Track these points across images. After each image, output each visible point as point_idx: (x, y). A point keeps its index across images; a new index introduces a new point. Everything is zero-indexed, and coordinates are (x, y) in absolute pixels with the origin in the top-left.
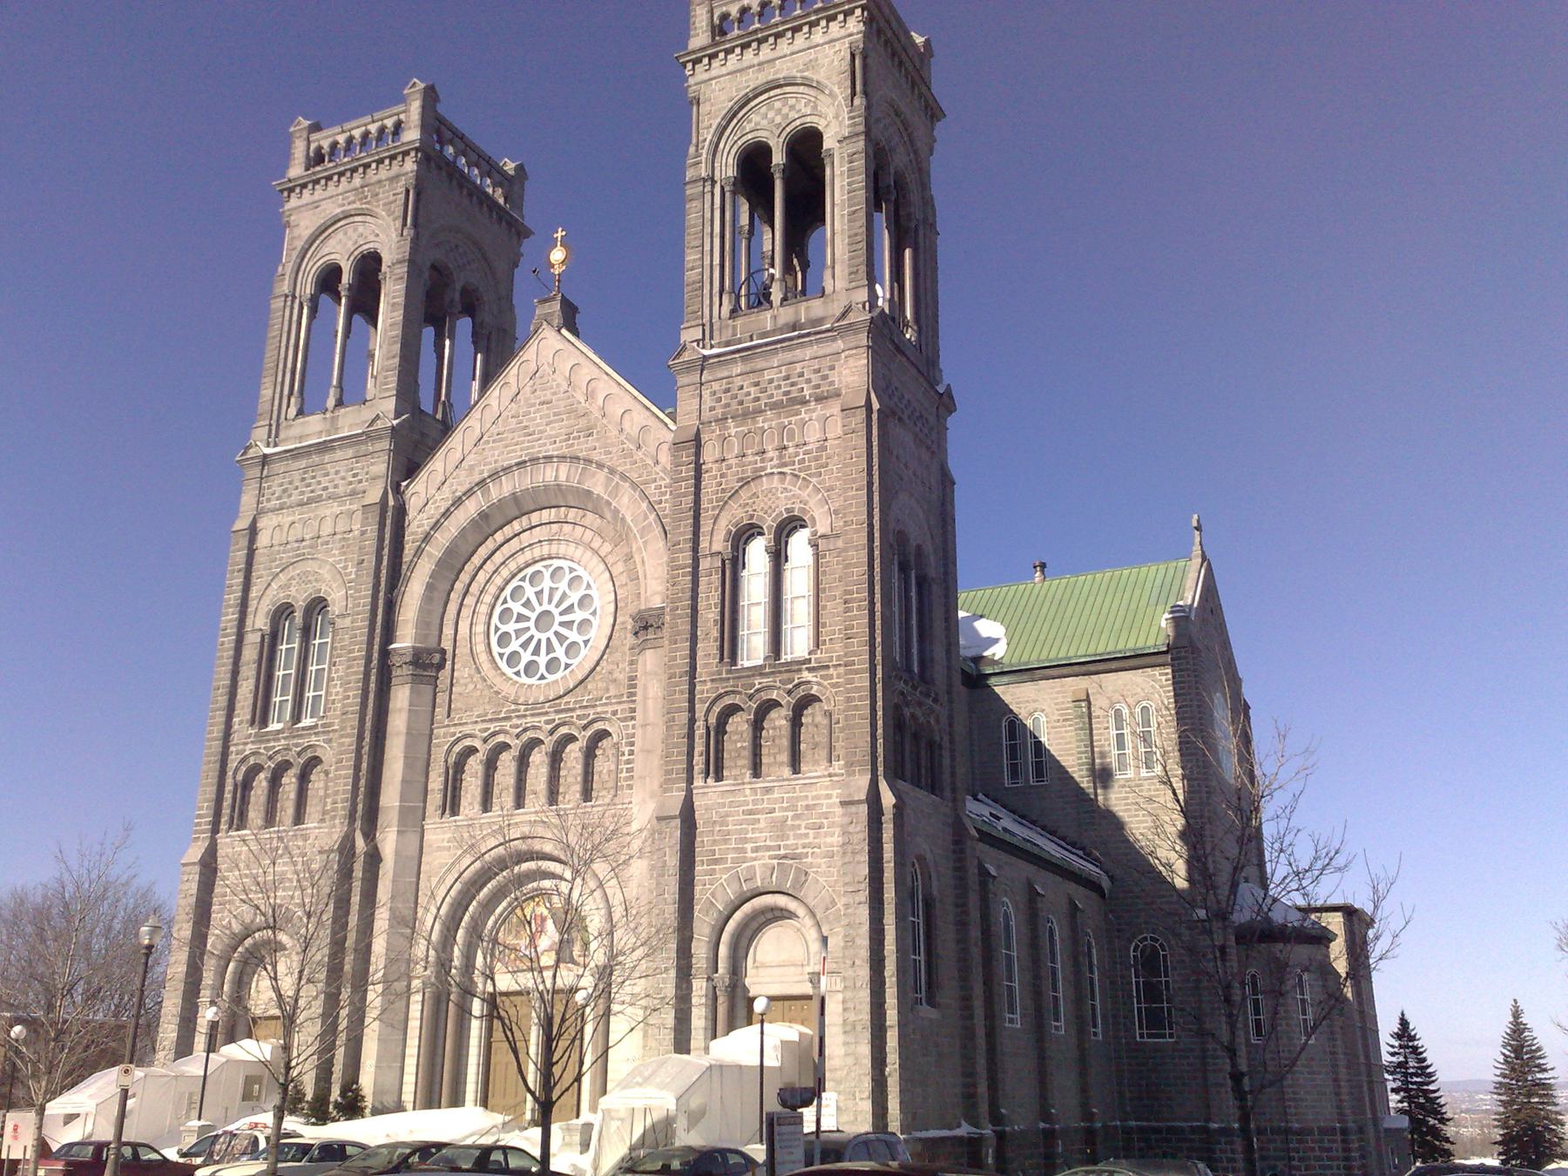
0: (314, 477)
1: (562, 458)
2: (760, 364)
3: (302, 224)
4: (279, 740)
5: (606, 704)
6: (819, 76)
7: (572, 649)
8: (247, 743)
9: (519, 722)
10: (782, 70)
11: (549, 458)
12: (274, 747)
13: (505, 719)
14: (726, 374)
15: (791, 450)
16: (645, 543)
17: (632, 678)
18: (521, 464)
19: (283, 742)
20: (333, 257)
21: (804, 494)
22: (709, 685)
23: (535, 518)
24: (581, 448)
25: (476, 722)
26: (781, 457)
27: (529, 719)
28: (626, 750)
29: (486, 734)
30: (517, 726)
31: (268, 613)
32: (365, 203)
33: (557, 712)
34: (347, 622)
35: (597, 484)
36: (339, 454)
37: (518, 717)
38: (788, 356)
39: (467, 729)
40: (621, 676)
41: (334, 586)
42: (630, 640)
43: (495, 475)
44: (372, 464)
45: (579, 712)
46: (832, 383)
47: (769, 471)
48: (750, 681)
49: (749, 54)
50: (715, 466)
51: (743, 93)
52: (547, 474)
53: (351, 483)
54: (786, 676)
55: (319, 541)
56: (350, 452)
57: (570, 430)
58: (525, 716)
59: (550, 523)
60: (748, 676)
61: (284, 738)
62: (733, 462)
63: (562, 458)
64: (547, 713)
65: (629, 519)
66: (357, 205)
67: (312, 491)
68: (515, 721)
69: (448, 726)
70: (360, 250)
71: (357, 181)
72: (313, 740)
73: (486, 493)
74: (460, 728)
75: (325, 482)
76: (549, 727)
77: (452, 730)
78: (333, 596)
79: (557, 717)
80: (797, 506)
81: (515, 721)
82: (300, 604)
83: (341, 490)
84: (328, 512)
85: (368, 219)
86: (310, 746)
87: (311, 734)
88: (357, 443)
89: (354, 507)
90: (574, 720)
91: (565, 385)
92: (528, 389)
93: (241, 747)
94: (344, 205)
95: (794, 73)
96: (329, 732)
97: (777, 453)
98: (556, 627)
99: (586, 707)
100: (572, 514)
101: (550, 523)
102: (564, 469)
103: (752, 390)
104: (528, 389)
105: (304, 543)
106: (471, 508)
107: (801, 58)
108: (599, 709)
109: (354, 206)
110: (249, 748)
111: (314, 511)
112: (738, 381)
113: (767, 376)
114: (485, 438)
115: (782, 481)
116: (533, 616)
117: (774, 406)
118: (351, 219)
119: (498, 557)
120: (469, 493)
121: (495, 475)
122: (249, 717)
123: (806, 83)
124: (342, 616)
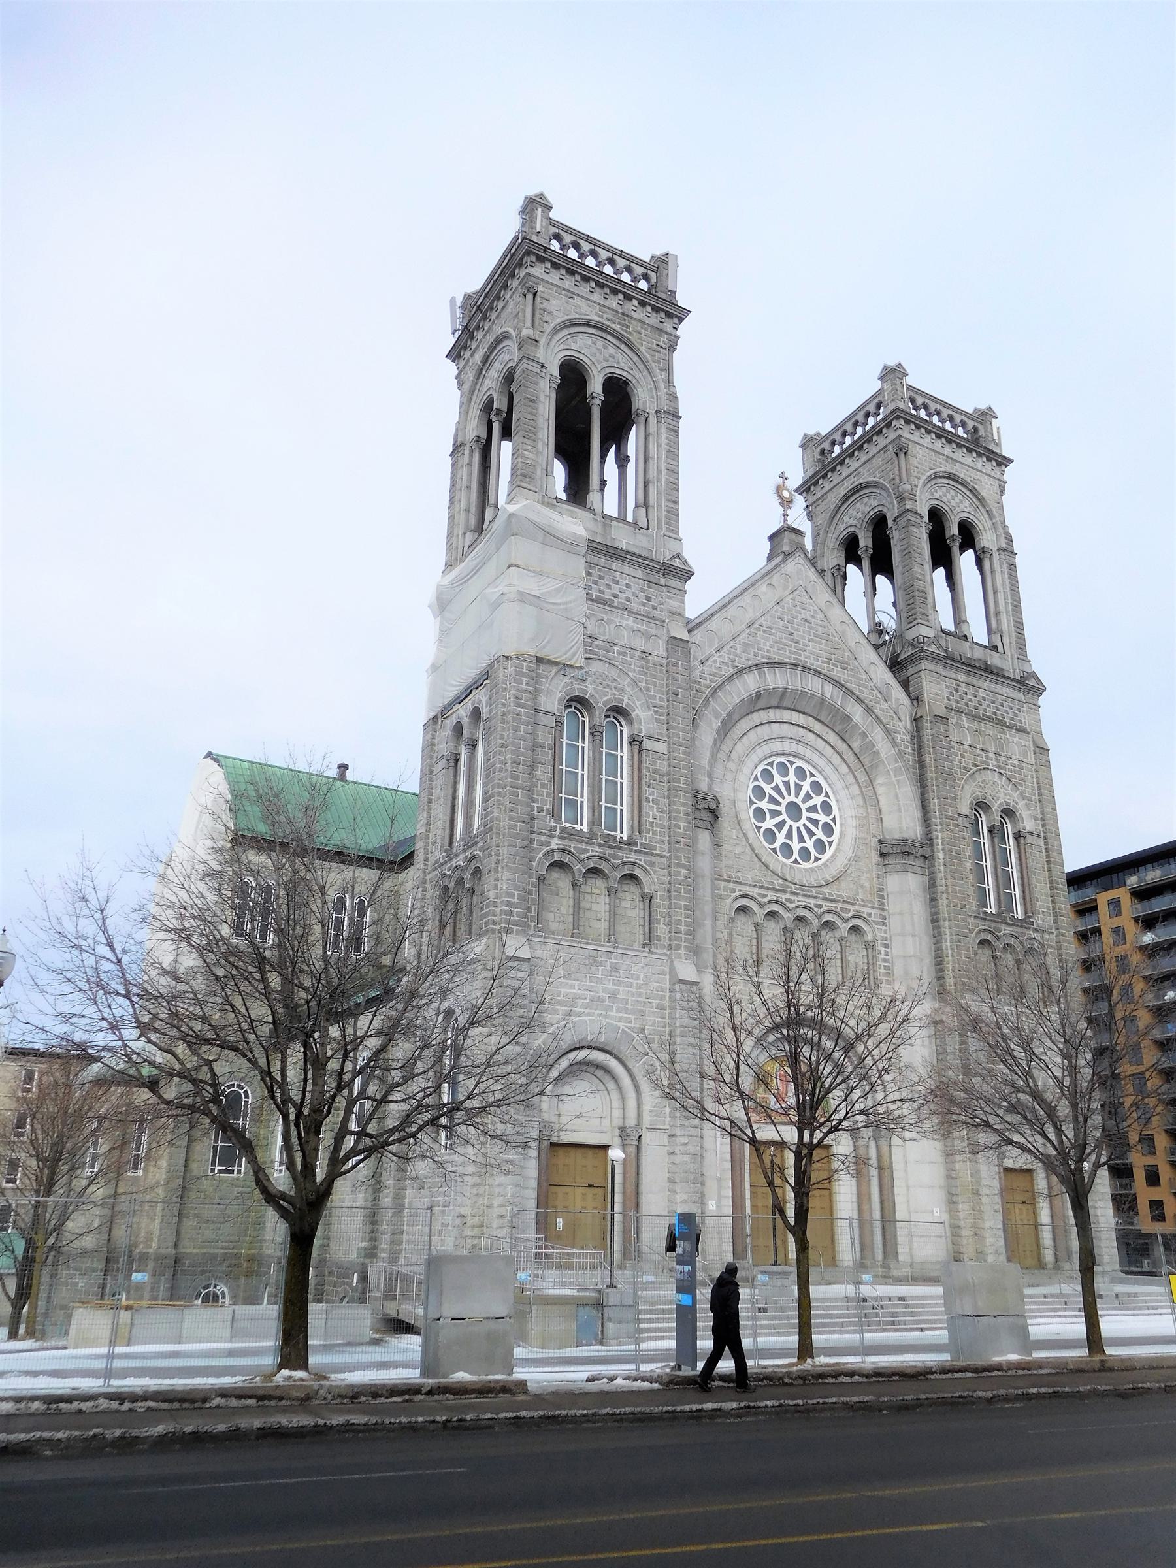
0: (601, 578)
1: (828, 679)
2: (976, 682)
3: (554, 302)
4: (593, 844)
5: (864, 906)
6: (984, 493)
7: (770, 835)
8: (554, 836)
9: (793, 898)
10: (962, 473)
11: (817, 673)
12: (587, 851)
13: (781, 891)
14: (954, 676)
15: (1003, 758)
16: (898, 781)
17: (881, 890)
18: (794, 665)
19: (597, 848)
20: (581, 357)
21: (1016, 795)
22: (972, 920)
23: (787, 715)
24: (837, 673)
25: (755, 886)
26: (997, 760)
27: (800, 898)
28: (883, 950)
29: (766, 900)
30: (791, 901)
31: (560, 700)
32: (626, 331)
33: (825, 899)
34: (661, 747)
35: (857, 713)
36: (626, 568)
37: (792, 893)
38: (994, 687)
39: (747, 890)
40: (867, 884)
41: (638, 703)
42: (875, 857)
43: (773, 664)
44: (668, 597)
45: (840, 905)
46: (1020, 722)
47: (990, 767)
48: (999, 925)
49: (938, 444)
50: (956, 745)
51: (938, 470)
52: (815, 685)
53: (644, 605)
54: (1019, 930)
55: (616, 649)
56: (639, 573)
57: (829, 656)
58: (797, 894)
59: (798, 725)
60: (998, 922)
61: (600, 845)
62: (968, 749)
63: (828, 679)
64: (815, 897)
65: (883, 755)
66: (617, 327)
67: (601, 592)
68: (788, 896)
69: (729, 881)
70: (613, 370)
71: (613, 302)
72: (633, 857)
73: (762, 675)
74: (738, 887)
75: (615, 588)
76: (819, 911)
77: (731, 885)
78: (637, 711)
79: (824, 904)
80: (1012, 803)
81: (788, 896)
82: (601, 702)
83: (634, 606)
84: (624, 623)
85: (623, 346)
86: (630, 863)
87: (631, 851)
88: (651, 568)
89: (653, 631)
90: (839, 910)
91: (821, 616)
92: (788, 599)
93: (543, 838)
94: (602, 317)
95: (968, 479)
96: (652, 854)
97: (994, 756)
98: (784, 816)
99: (848, 903)
100: (817, 727)
101: (798, 725)
102: (829, 690)
103: (973, 698)
104: (788, 599)
105: (596, 642)
106: (751, 683)
107: (978, 476)
108: (857, 908)
109: (613, 326)
110: (555, 843)
111: (606, 614)
112: (963, 688)
113: (981, 693)
114: (756, 625)
115: (1000, 779)
116: (803, 807)
117: (990, 719)
118: (604, 335)
119: (753, 736)
120: (750, 668)
121: (773, 664)
122: (549, 806)
123: (974, 492)
124: (654, 739)
